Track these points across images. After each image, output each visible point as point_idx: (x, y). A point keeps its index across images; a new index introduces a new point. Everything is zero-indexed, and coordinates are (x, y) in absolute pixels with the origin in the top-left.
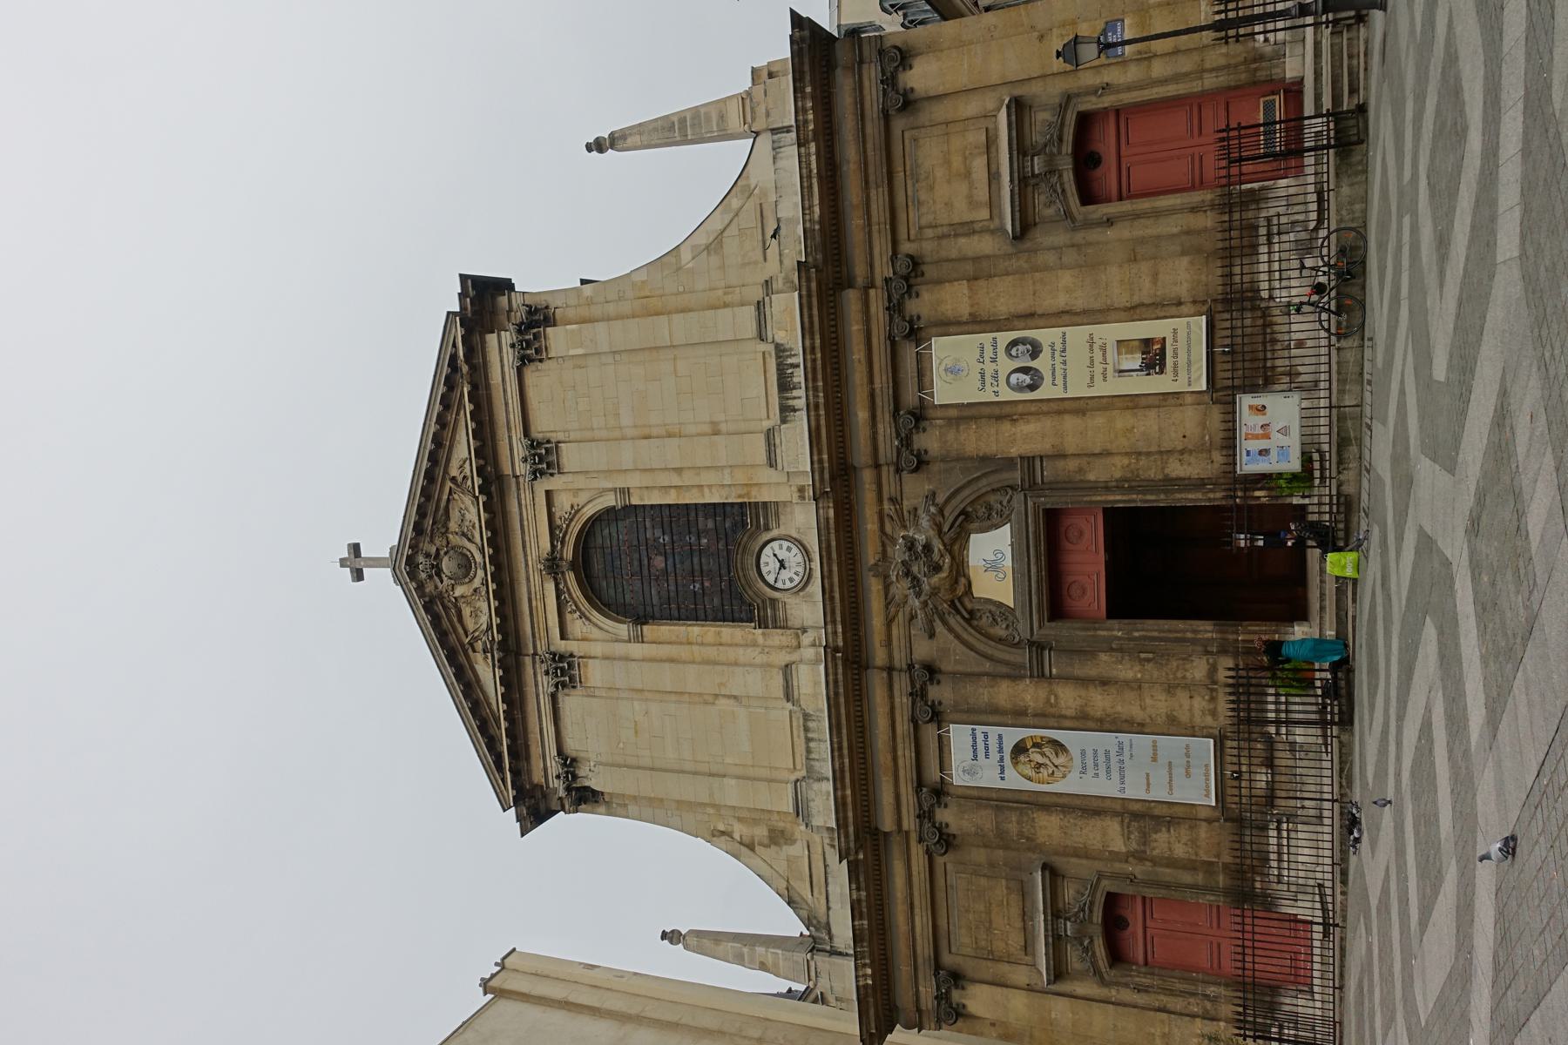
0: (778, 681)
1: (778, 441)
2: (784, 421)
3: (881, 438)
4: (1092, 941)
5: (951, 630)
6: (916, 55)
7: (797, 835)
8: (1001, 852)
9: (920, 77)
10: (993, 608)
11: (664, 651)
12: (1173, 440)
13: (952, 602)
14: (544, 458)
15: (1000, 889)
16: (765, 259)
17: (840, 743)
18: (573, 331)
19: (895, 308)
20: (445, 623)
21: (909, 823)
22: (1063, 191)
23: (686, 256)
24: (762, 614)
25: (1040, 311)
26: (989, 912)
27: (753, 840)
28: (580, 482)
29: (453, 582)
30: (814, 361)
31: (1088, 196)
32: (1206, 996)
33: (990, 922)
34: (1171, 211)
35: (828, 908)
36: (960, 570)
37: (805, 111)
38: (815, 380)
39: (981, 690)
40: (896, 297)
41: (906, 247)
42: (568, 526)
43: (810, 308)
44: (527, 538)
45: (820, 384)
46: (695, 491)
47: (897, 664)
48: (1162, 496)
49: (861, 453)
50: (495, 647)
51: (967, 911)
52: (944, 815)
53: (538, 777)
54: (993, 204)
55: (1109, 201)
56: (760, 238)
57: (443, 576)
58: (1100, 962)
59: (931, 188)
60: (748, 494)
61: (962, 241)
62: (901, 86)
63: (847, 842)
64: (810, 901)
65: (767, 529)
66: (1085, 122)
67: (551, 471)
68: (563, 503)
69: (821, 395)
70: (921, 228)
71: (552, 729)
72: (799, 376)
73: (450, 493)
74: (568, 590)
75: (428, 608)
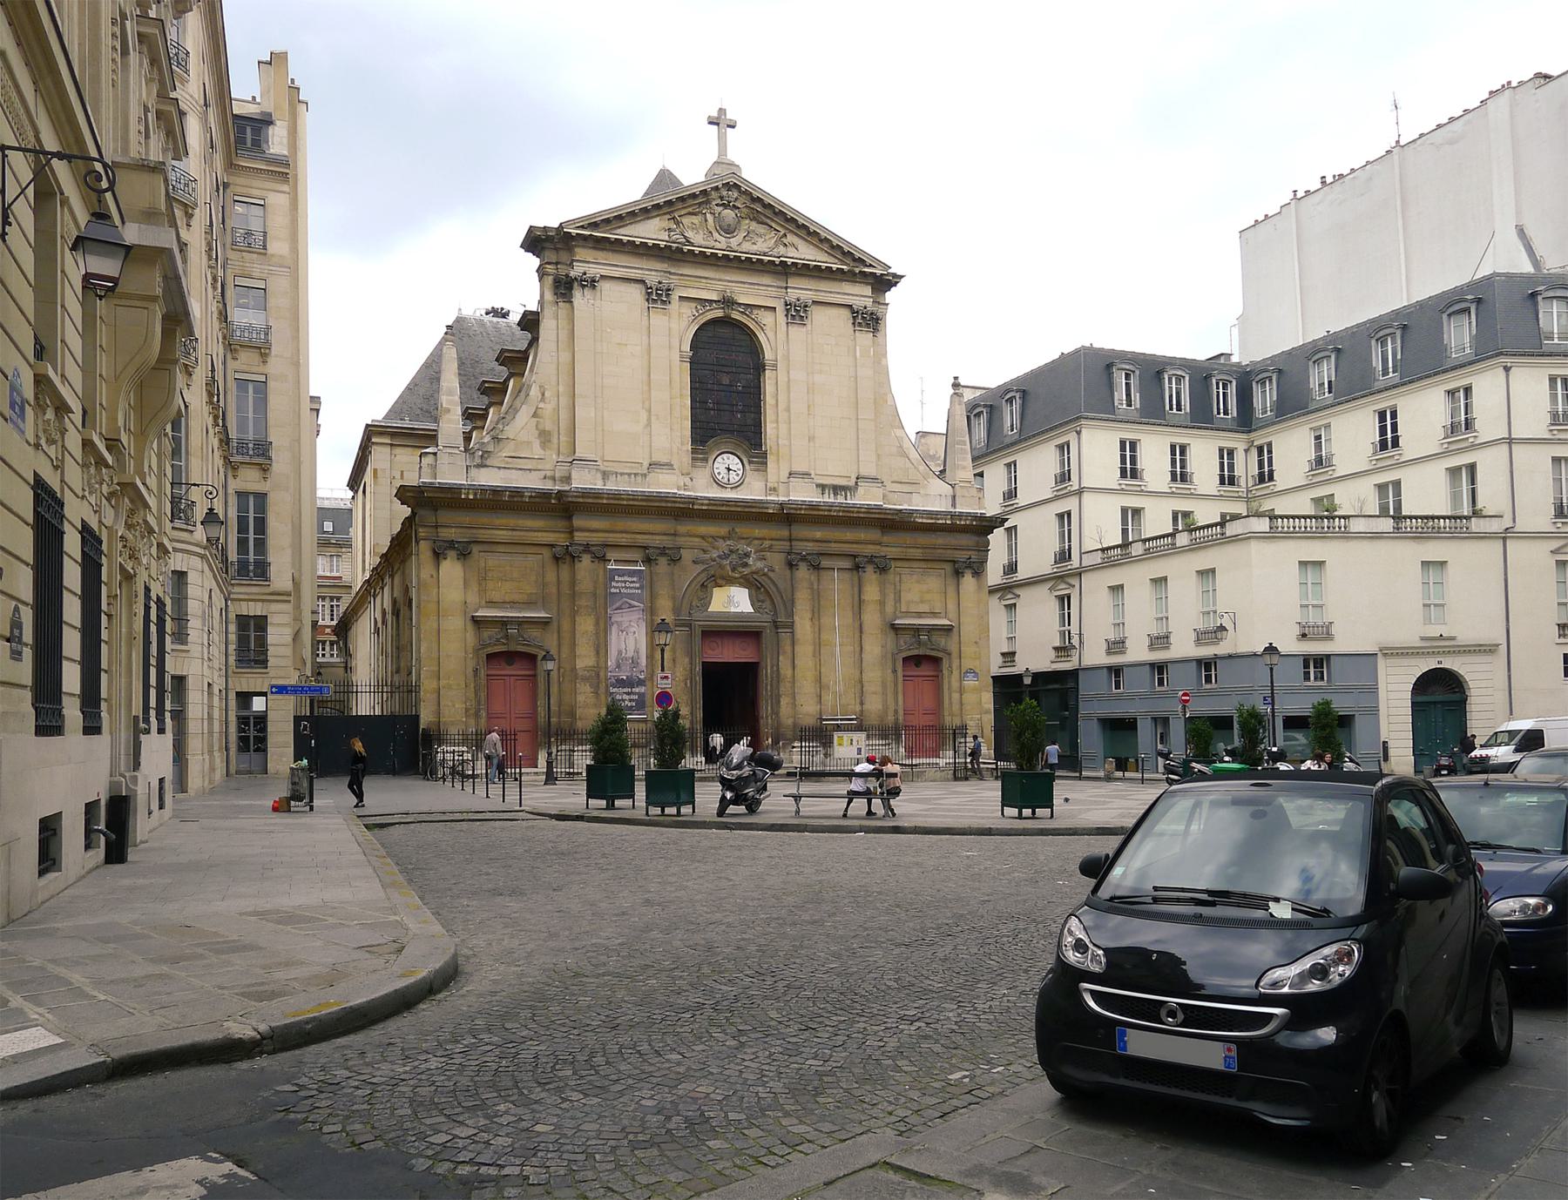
0: (664, 459)
1: (806, 480)
2: (818, 486)
3: (806, 544)
4: (504, 644)
5: (699, 573)
6: (978, 580)
7: (548, 452)
8: (554, 590)
9: (968, 581)
10: (708, 599)
11: (676, 378)
12: (800, 699)
13: (713, 576)
14: (797, 313)
15: (529, 589)
16: (892, 482)
17: (637, 500)
18: (869, 351)
19: (871, 559)
20: (691, 202)
21: (579, 537)
22: (910, 650)
23: (899, 432)
24: (700, 451)
25: (863, 637)
26: (512, 580)
27: (540, 418)
28: (781, 335)
29: (717, 215)
30: (853, 512)
31: (905, 660)
32: (479, 710)
33: (506, 580)
34: (897, 702)
35: (499, 468)
36: (730, 581)
37: (966, 520)
38: (843, 511)
39: (666, 590)
40: (876, 560)
41: (893, 564)
42: (753, 319)
43: (879, 513)
44: (746, 286)
45: (841, 514)
46: (774, 418)
47: (678, 538)
48: (769, 693)
49: (801, 531)
50: (680, 246)
51: (511, 566)
52: (586, 560)
53: (581, 253)
54: (908, 614)
55: (903, 671)
56: (903, 481)
57: (721, 208)
58: (489, 649)
59: (918, 582)
60: (771, 453)
61: (892, 596)
62: (966, 571)
63: (572, 497)
64: (499, 454)
65: (750, 462)
66: (936, 661)
67: (790, 316)
68: (766, 318)
69: (835, 514)
70: (900, 574)
71: (617, 275)
72: (840, 499)
73: (775, 230)
74: (712, 310)
75: (704, 192)
